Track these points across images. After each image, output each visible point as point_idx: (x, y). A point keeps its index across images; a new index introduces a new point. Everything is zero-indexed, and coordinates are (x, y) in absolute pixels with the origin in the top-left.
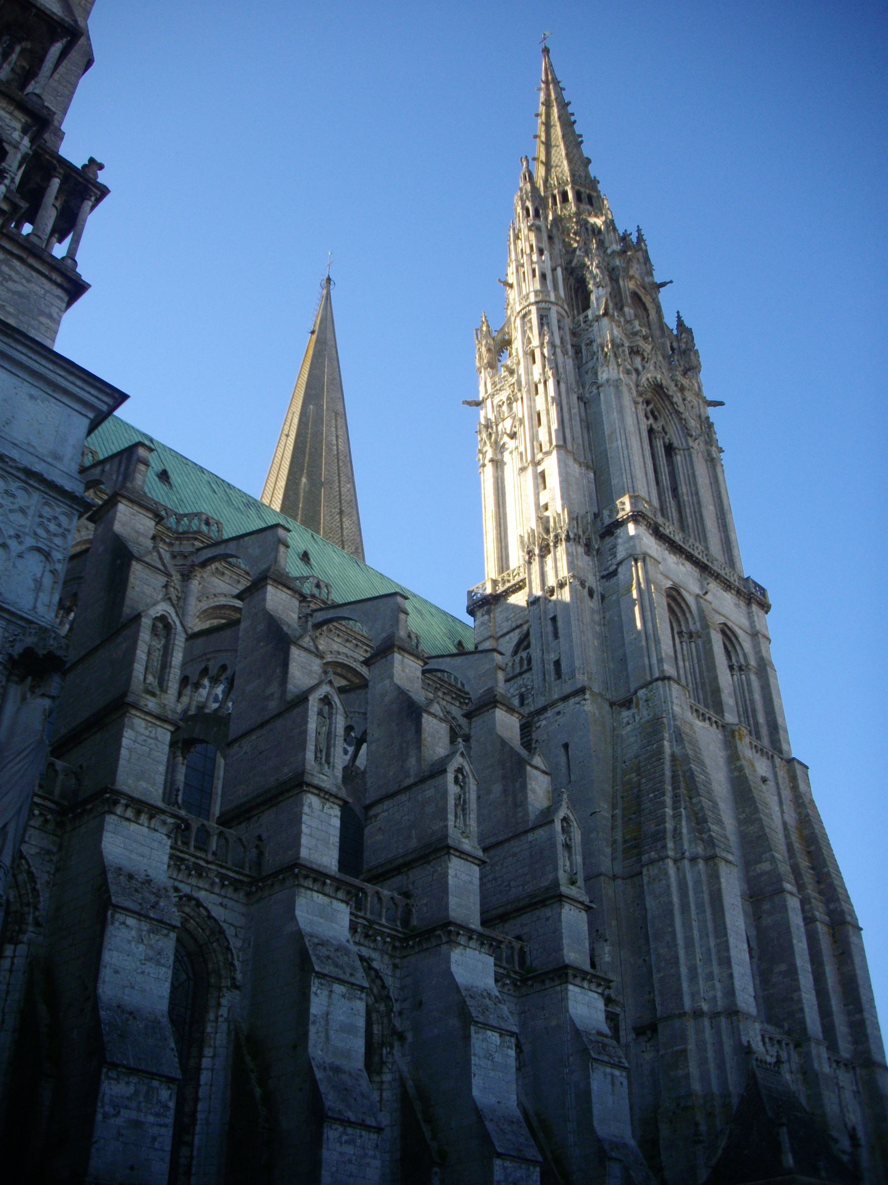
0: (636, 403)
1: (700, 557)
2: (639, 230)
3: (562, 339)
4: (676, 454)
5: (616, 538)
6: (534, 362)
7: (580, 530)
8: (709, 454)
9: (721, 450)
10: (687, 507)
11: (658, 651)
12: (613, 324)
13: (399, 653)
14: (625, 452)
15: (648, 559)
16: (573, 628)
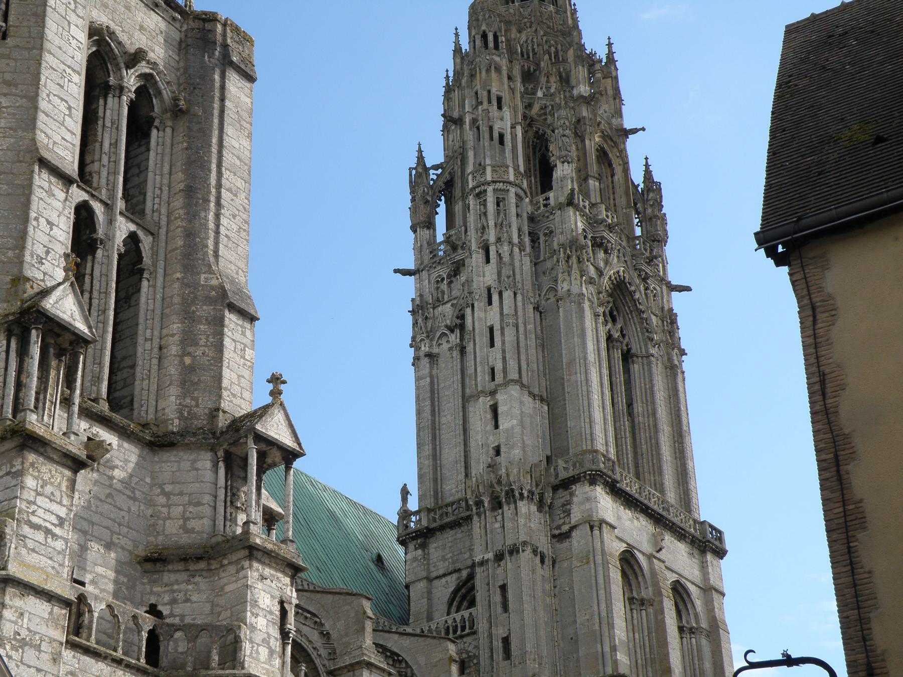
0: (596, 315)
1: (655, 507)
2: (610, 45)
3: (519, 230)
4: (633, 362)
5: (572, 495)
6: (488, 261)
7: (534, 484)
8: (670, 359)
9: (683, 353)
10: (642, 431)
11: (612, 637)
12: (578, 213)
13: (368, 669)
14: (584, 389)
15: (604, 525)
16: (526, 606)
